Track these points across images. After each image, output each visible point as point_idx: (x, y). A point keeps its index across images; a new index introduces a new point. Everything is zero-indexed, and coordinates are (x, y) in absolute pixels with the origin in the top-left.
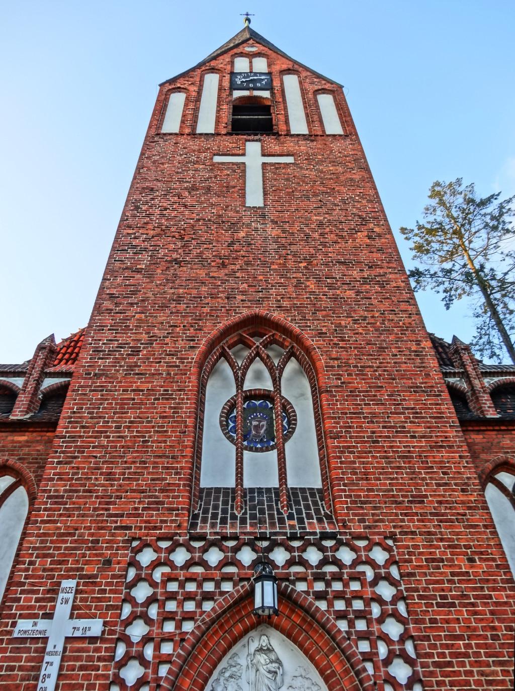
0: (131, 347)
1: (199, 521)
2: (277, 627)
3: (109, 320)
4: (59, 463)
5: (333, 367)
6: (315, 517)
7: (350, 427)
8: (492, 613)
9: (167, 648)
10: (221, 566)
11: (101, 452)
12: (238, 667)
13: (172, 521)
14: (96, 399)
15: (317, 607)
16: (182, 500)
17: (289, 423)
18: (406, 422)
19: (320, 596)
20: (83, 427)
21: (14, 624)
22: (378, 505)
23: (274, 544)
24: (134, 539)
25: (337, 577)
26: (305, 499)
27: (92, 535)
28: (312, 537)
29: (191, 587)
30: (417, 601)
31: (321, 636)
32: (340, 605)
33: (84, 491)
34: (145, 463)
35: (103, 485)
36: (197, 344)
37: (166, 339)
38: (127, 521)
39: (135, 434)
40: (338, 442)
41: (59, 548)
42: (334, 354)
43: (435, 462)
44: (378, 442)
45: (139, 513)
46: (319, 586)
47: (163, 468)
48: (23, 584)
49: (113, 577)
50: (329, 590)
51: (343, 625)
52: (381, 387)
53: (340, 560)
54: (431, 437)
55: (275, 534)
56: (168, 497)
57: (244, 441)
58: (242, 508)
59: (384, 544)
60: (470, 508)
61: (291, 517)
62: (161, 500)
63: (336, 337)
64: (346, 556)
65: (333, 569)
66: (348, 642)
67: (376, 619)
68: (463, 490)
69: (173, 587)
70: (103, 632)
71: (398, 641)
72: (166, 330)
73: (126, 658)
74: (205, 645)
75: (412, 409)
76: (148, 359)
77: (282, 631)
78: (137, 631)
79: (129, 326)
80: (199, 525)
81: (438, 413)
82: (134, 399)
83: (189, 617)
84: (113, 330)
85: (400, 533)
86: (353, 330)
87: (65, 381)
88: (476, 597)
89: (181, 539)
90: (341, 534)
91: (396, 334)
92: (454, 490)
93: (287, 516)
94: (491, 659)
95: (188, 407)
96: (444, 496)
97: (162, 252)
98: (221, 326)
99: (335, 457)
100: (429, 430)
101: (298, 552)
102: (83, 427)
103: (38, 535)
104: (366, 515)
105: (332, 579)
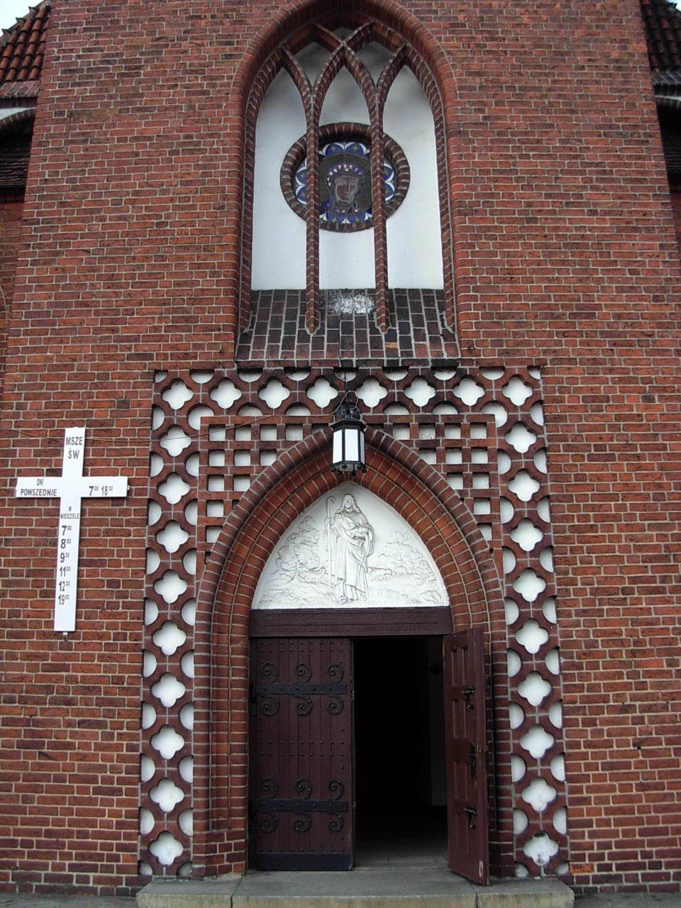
0: (125, 61)
1: (251, 345)
2: (366, 485)
3: (82, 11)
4: (34, 263)
5: (471, 88)
6: (428, 337)
7: (493, 195)
8: (662, 467)
9: (217, 512)
10: (285, 407)
11: (94, 244)
12: (313, 532)
13: (211, 346)
14: (78, 157)
15: (421, 460)
16: (222, 314)
17: (397, 182)
18: (584, 188)
19: (427, 447)
20: (62, 204)
21: (14, 483)
22: (525, 320)
23: (364, 379)
24: (157, 372)
25: (452, 423)
26: (417, 308)
27: (97, 367)
28: (420, 367)
29: (245, 436)
30: (562, 452)
31: (426, 496)
32: (455, 459)
33: (78, 304)
34: (163, 258)
35: (104, 295)
36: (236, 49)
37: (184, 43)
38: (144, 347)
39: (144, 212)
40: (471, 221)
41: (54, 387)
42: (475, 65)
43: (621, 254)
44: (535, 220)
45: (161, 336)
46: (428, 435)
47: (192, 266)
48: (15, 434)
49: (134, 423)
50: (441, 439)
51: (457, 484)
52: (551, 126)
53: (460, 399)
54: (621, 213)
55: (366, 362)
56: (203, 310)
57: (322, 213)
58: (316, 324)
59: (525, 377)
60: (661, 325)
61: (391, 337)
62: (192, 314)
63: (482, 32)
64: (470, 394)
65: (451, 411)
66: (461, 503)
67: (502, 475)
68: (656, 299)
69: (219, 436)
70: (129, 492)
71: (528, 502)
72: (183, 25)
73: (163, 523)
74: (267, 507)
75: (597, 165)
76: (155, 81)
77: (374, 490)
78: (175, 491)
79: (118, 21)
80: (251, 350)
81: (638, 172)
82: (137, 154)
83: (243, 474)
84: (91, 29)
85: (552, 361)
86: (513, 19)
87: (19, 113)
88: (644, 448)
89: (226, 372)
90: (464, 362)
91: (589, 27)
92: (642, 298)
93: (385, 335)
94: (646, 523)
95: (225, 163)
96: (625, 307)
98: (277, 14)
99: (463, 246)
100: (619, 201)
101: (398, 389)
102: (62, 204)
103: (23, 369)
104: (505, 334)
105: (445, 424)
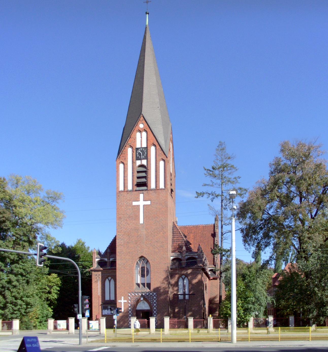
46: (148, 297)
97: (125, 240)
